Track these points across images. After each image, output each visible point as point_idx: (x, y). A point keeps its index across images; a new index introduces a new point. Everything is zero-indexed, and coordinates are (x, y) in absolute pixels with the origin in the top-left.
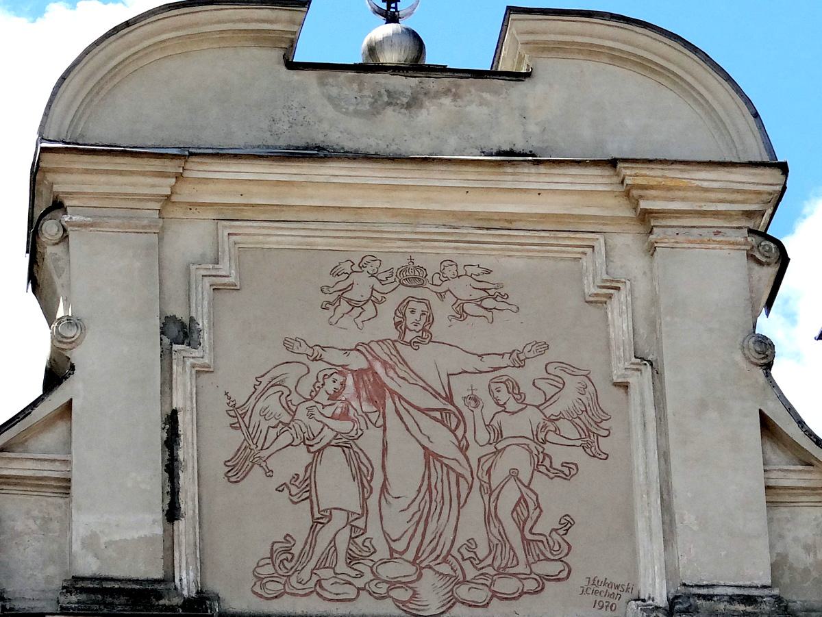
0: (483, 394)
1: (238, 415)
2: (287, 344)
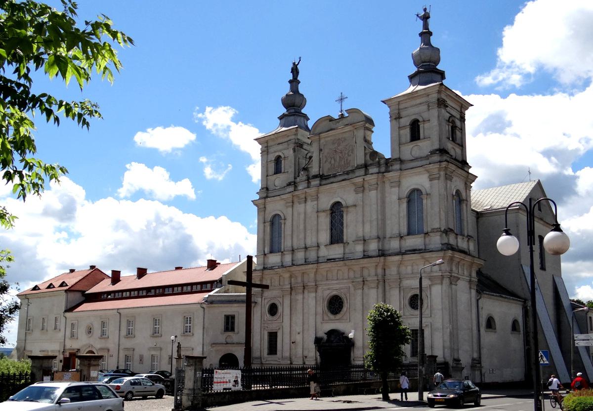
1: (326, 157)
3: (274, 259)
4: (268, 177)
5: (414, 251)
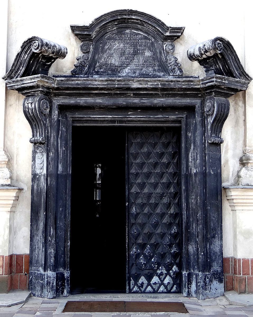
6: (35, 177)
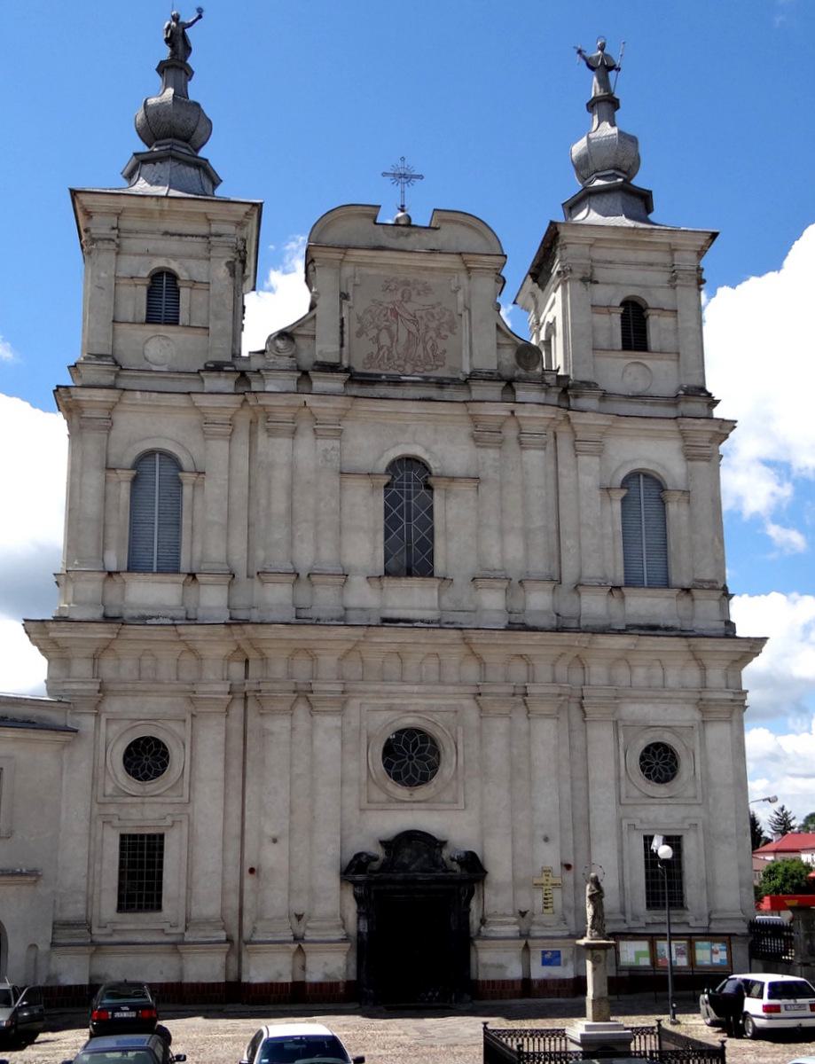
0: (424, 316)
1: (359, 319)
2: (373, 301)
3: (150, 592)
4: (120, 327)
5: (652, 629)
6: (359, 933)
